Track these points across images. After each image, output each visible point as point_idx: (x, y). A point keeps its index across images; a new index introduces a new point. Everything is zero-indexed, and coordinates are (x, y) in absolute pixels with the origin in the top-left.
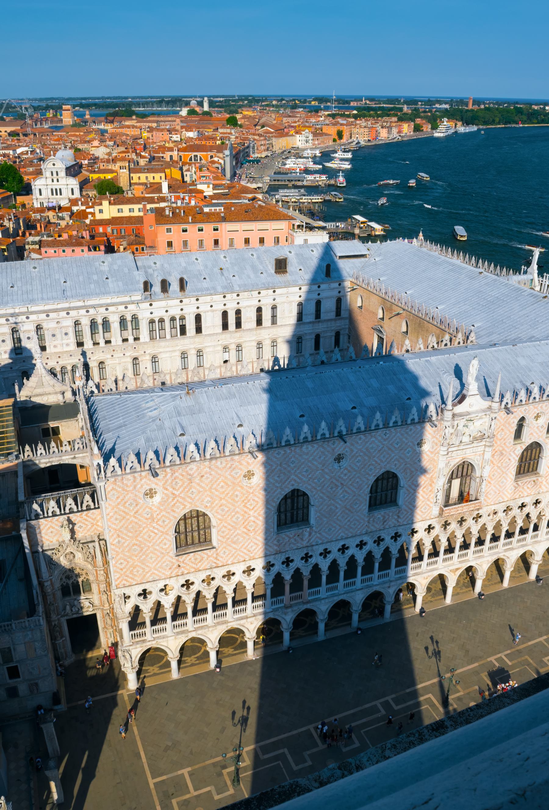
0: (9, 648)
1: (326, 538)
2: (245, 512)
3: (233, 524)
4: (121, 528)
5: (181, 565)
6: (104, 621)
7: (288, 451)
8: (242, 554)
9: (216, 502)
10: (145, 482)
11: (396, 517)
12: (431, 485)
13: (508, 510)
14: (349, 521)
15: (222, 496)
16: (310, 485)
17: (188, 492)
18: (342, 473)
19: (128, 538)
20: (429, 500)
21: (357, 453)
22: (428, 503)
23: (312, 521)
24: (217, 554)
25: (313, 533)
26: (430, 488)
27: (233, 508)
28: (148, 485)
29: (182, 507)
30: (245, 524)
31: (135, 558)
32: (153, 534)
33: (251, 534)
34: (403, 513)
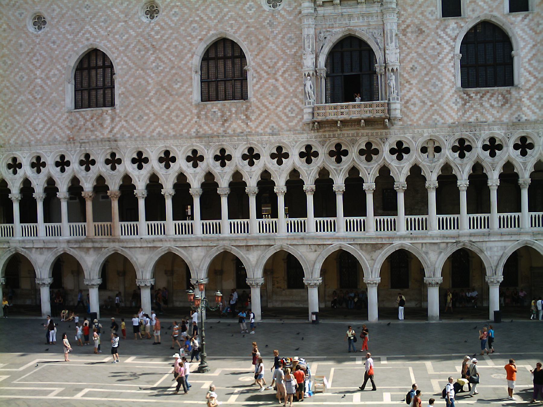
1: (137, 130)
2: (31, 71)
3: (17, 86)
8: (27, 133)
11: (244, 117)
12: (296, 70)
13: (462, 148)
14: (168, 108)
18: (152, 29)
20: (296, 96)
22: (297, 101)
23: (117, 101)
25: (117, 119)
26: (296, 75)
30: (32, 87)
33: (39, 105)
34: (253, 112)
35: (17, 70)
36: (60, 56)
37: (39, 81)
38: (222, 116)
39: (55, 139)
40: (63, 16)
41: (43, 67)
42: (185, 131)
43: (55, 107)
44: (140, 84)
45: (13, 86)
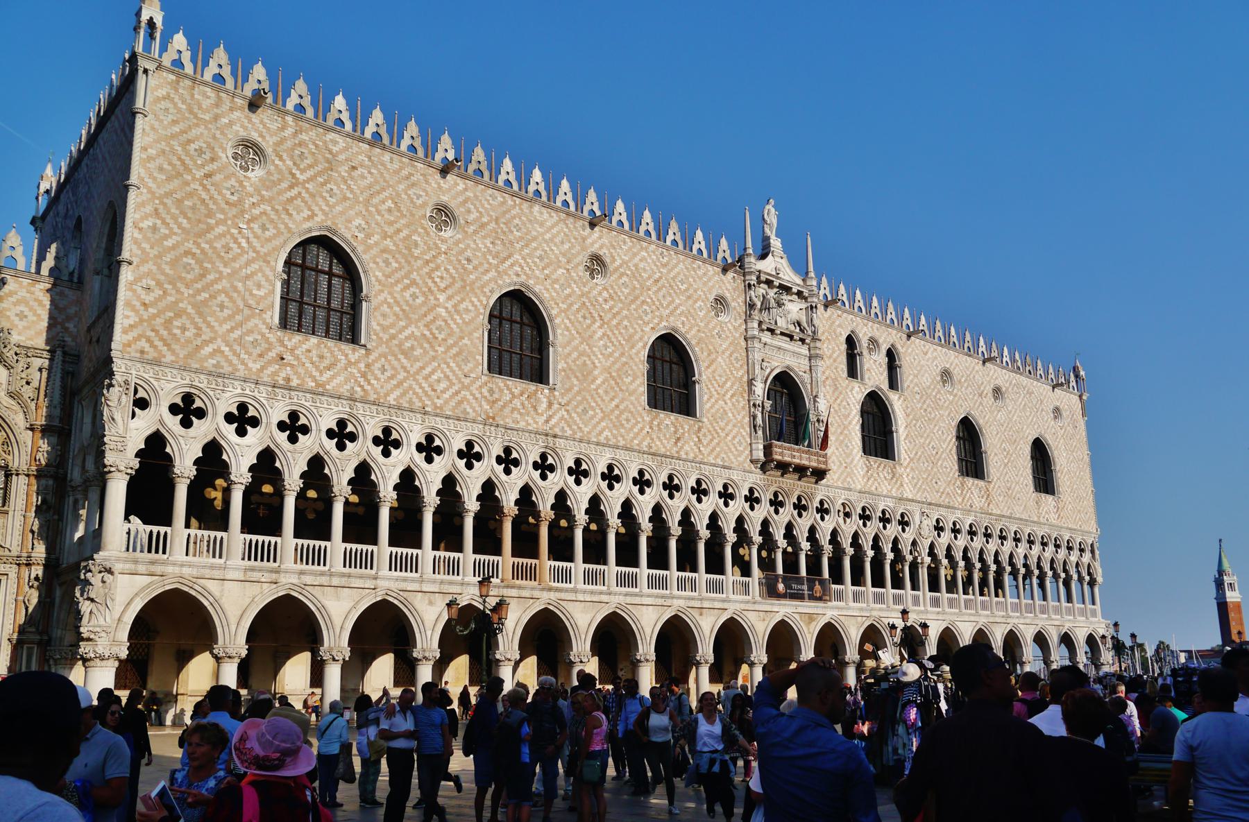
4: (168, 194)
5: (288, 357)
7: (510, 202)
9: (376, 238)
10: (239, 119)
14: (617, 406)
15: (390, 230)
16: (547, 290)
19: (176, 230)
21: (621, 266)
24: (368, 366)
25: (556, 406)
27: (407, 268)
28: (245, 128)
29: (307, 213)
30: (429, 318)
31: (183, 289)
32: (235, 246)
33: (441, 349)
34: (704, 435)
35: (407, 281)
36: (477, 284)
37: (442, 311)
38: (675, 432)
39: (465, 412)
40: (483, 226)
41: (450, 292)
42: (636, 442)
43: (466, 361)
44: (584, 364)
45: (400, 306)
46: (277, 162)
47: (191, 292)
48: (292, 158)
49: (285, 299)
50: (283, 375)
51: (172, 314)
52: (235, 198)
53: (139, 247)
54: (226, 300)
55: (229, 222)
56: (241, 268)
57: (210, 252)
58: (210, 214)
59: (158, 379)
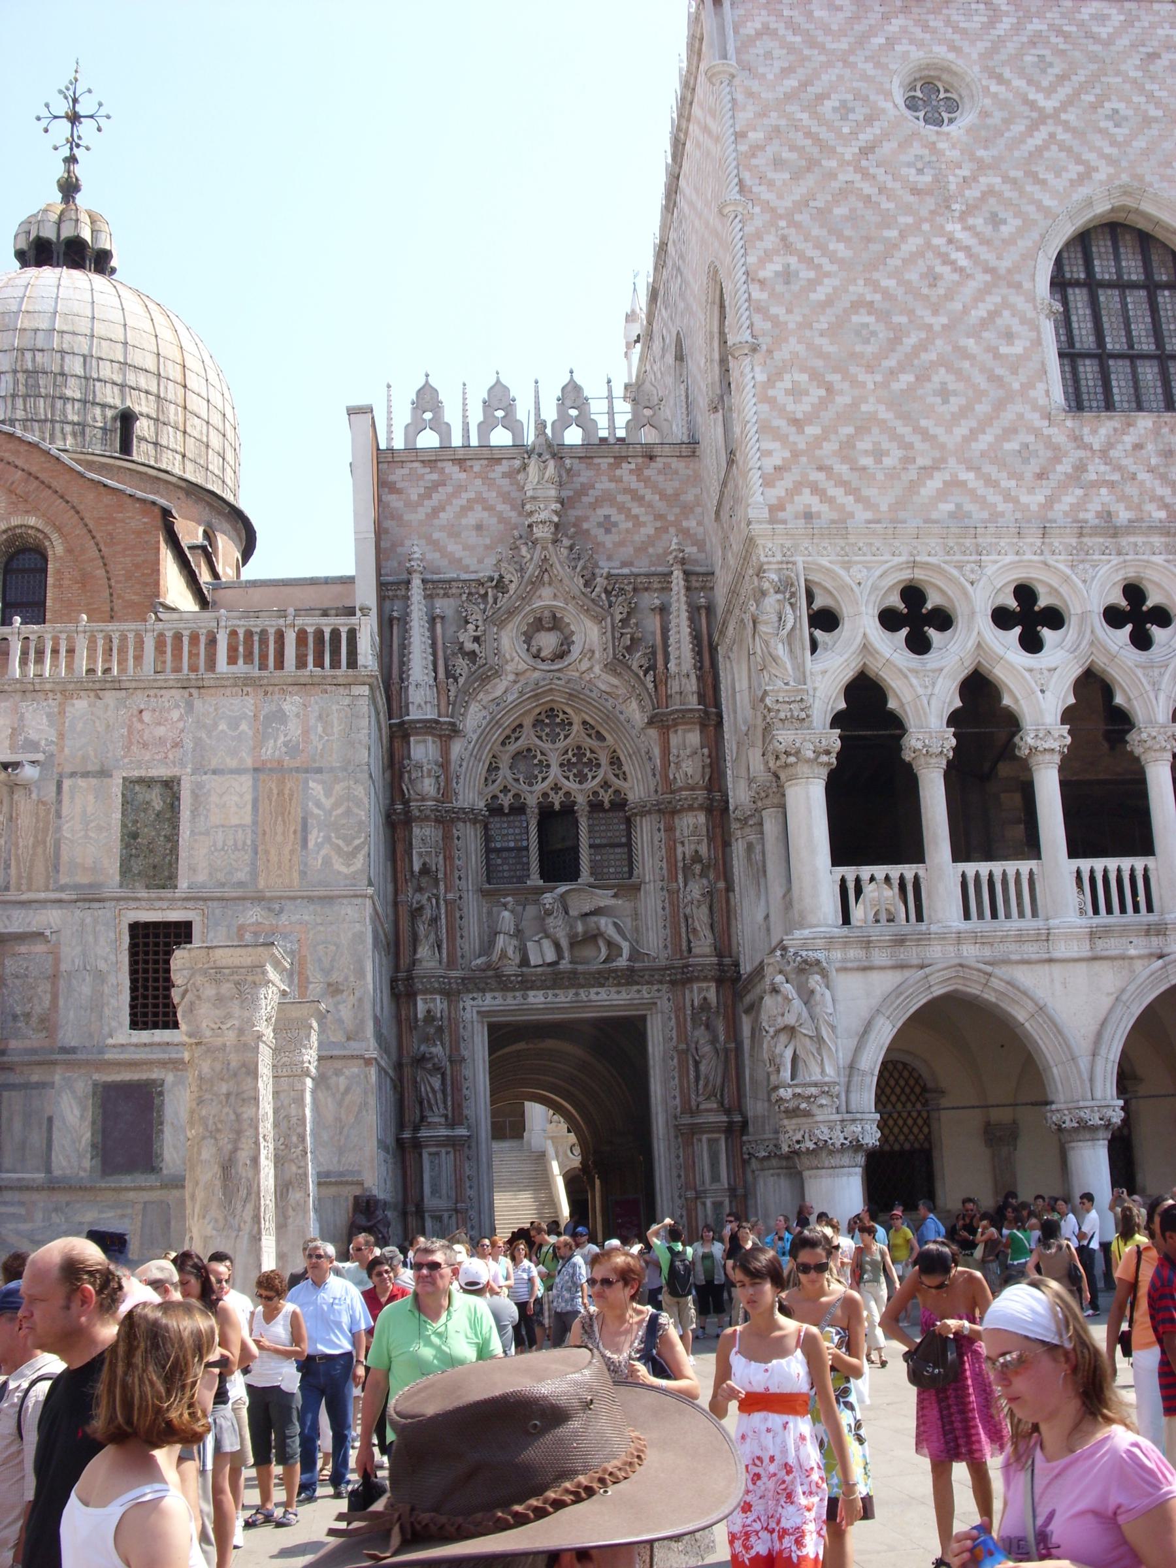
0: (170, 786)
6: (683, 1054)
10: (904, 30)
17: (1094, 107)
19: (828, 267)
29: (1075, 170)
32: (944, 270)
46: (994, 88)
47: (879, 378)
48: (1022, 73)
49: (1069, 355)
50: (1095, 506)
51: (850, 430)
52: (928, 178)
53: (767, 316)
54: (949, 378)
55: (926, 227)
56: (966, 311)
57: (900, 292)
58: (887, 221)
59: (847, 566)
